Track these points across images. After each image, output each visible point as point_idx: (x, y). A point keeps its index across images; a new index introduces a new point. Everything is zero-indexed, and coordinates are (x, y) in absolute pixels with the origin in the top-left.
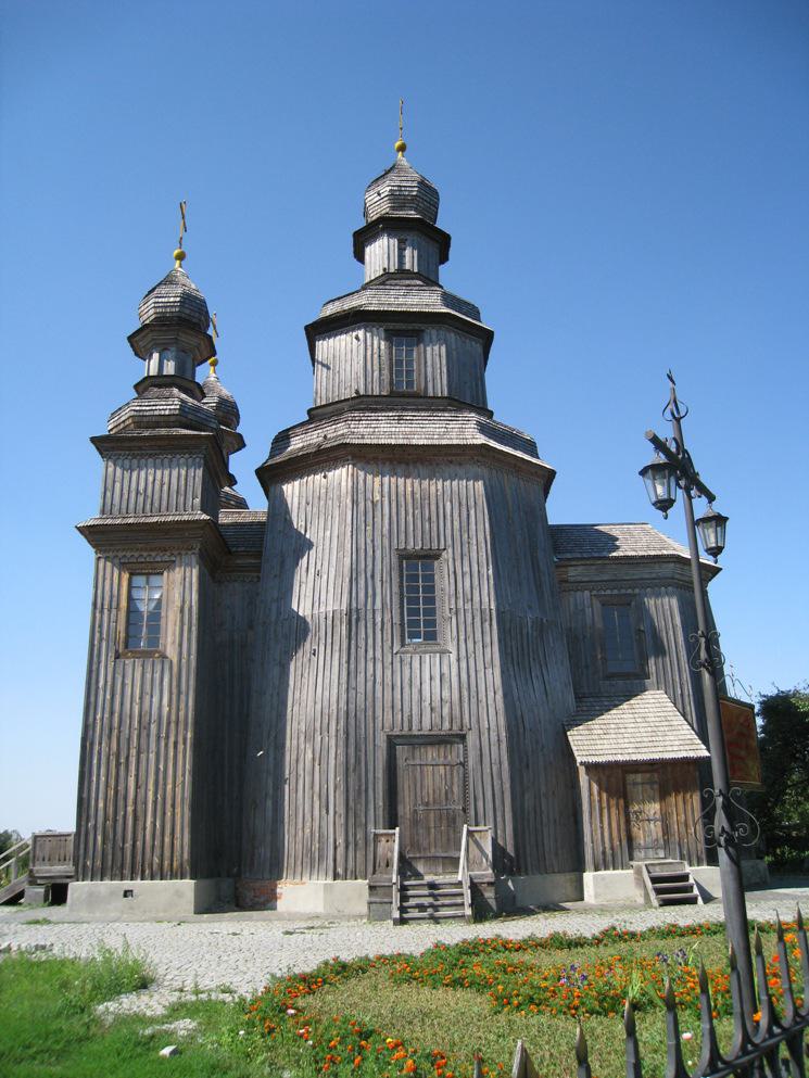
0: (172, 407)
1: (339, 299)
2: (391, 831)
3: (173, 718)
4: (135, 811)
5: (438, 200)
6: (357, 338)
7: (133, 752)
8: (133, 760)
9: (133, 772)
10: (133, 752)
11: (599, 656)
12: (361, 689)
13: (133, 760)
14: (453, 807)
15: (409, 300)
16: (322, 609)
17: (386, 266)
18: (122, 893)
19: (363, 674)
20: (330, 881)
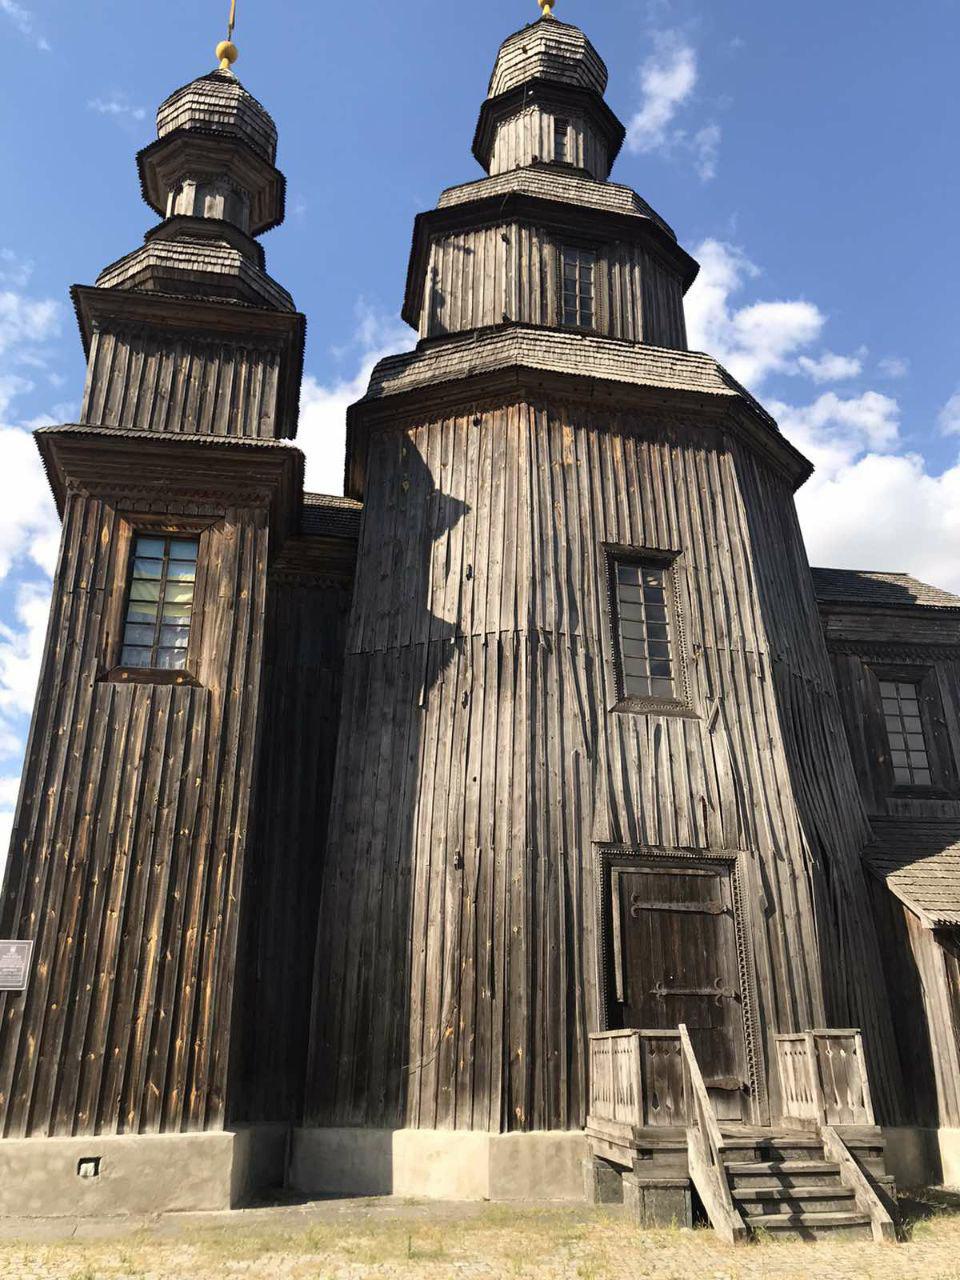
0: (228, 262)
1: (476, 182)
2: (670, 1033)
3: (210, 800)
4: (117, 983)
5: (607, 78)
6: (506, 239)
7: (122, 862)
8: (121, 878)
9: (119, 901)
10: (122, 862)
11: (881, 759)
12: (555, 767)
13: (121, 878)
14: (718, 992)
15: (586, 197)
16: (480, 630)
17: (537, 154)
18: (78, 1161)
19: (557, 740)
20: (495, 1133)
